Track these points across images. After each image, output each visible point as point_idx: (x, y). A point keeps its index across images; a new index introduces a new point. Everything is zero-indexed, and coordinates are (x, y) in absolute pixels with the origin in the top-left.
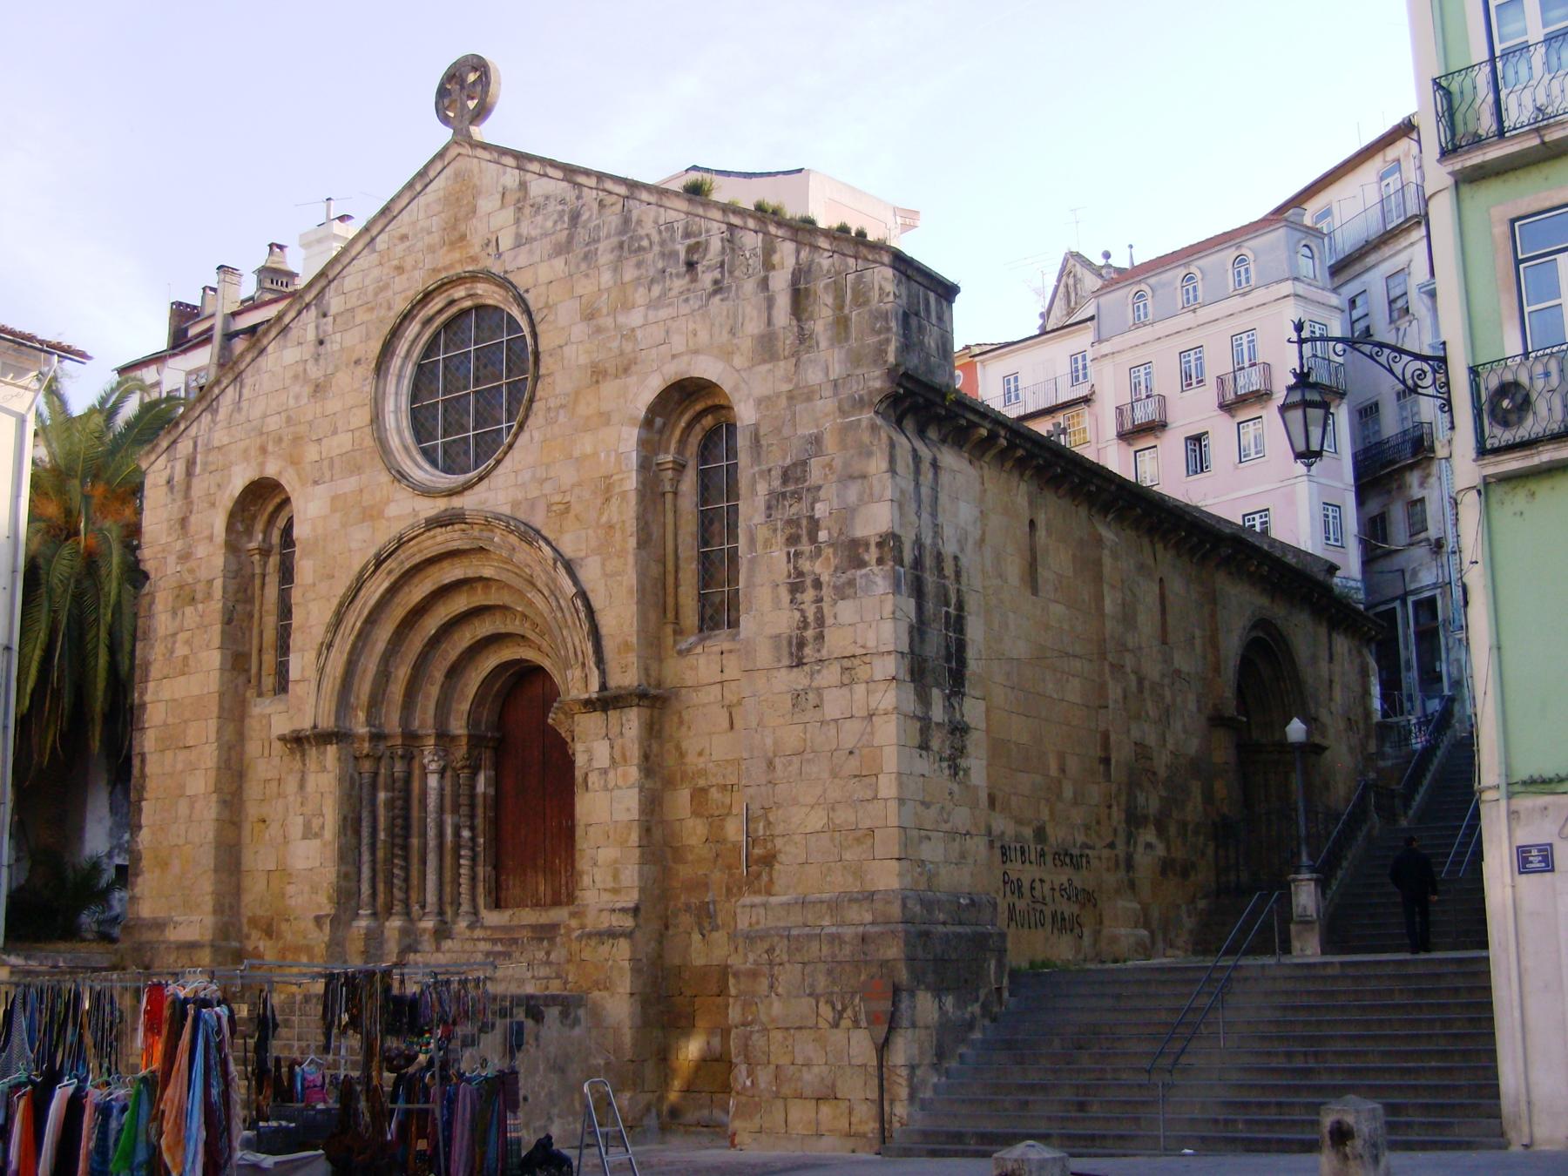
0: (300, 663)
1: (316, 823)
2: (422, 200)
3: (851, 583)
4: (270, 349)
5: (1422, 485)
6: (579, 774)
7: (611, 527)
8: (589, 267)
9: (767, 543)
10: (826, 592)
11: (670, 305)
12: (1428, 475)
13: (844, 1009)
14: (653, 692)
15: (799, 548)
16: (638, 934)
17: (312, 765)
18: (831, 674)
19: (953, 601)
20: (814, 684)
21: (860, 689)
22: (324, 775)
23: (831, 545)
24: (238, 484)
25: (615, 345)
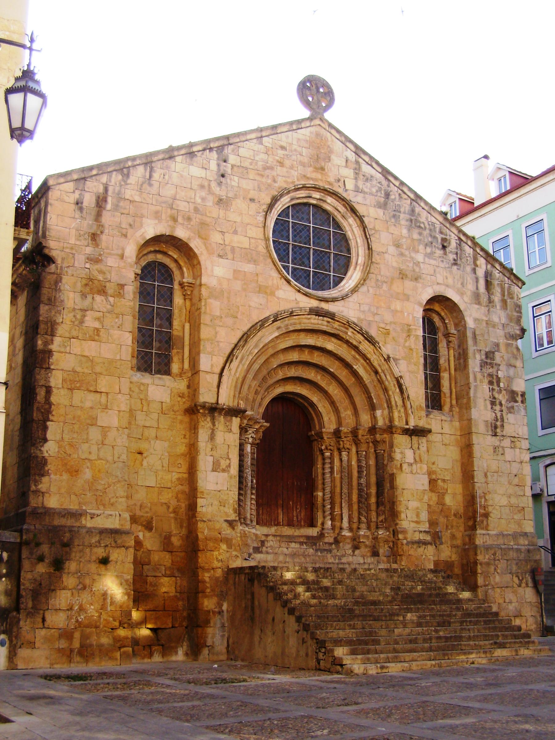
1: (224, 464)
2: (294, 133)
3: (513, 407)
7: (411, 349)
8: (396, 221)
9: (481, 381)
11: (435, 259)
13: (523, 579)
18: (507, 443)
20: (501, 445)
21: (517, 450)
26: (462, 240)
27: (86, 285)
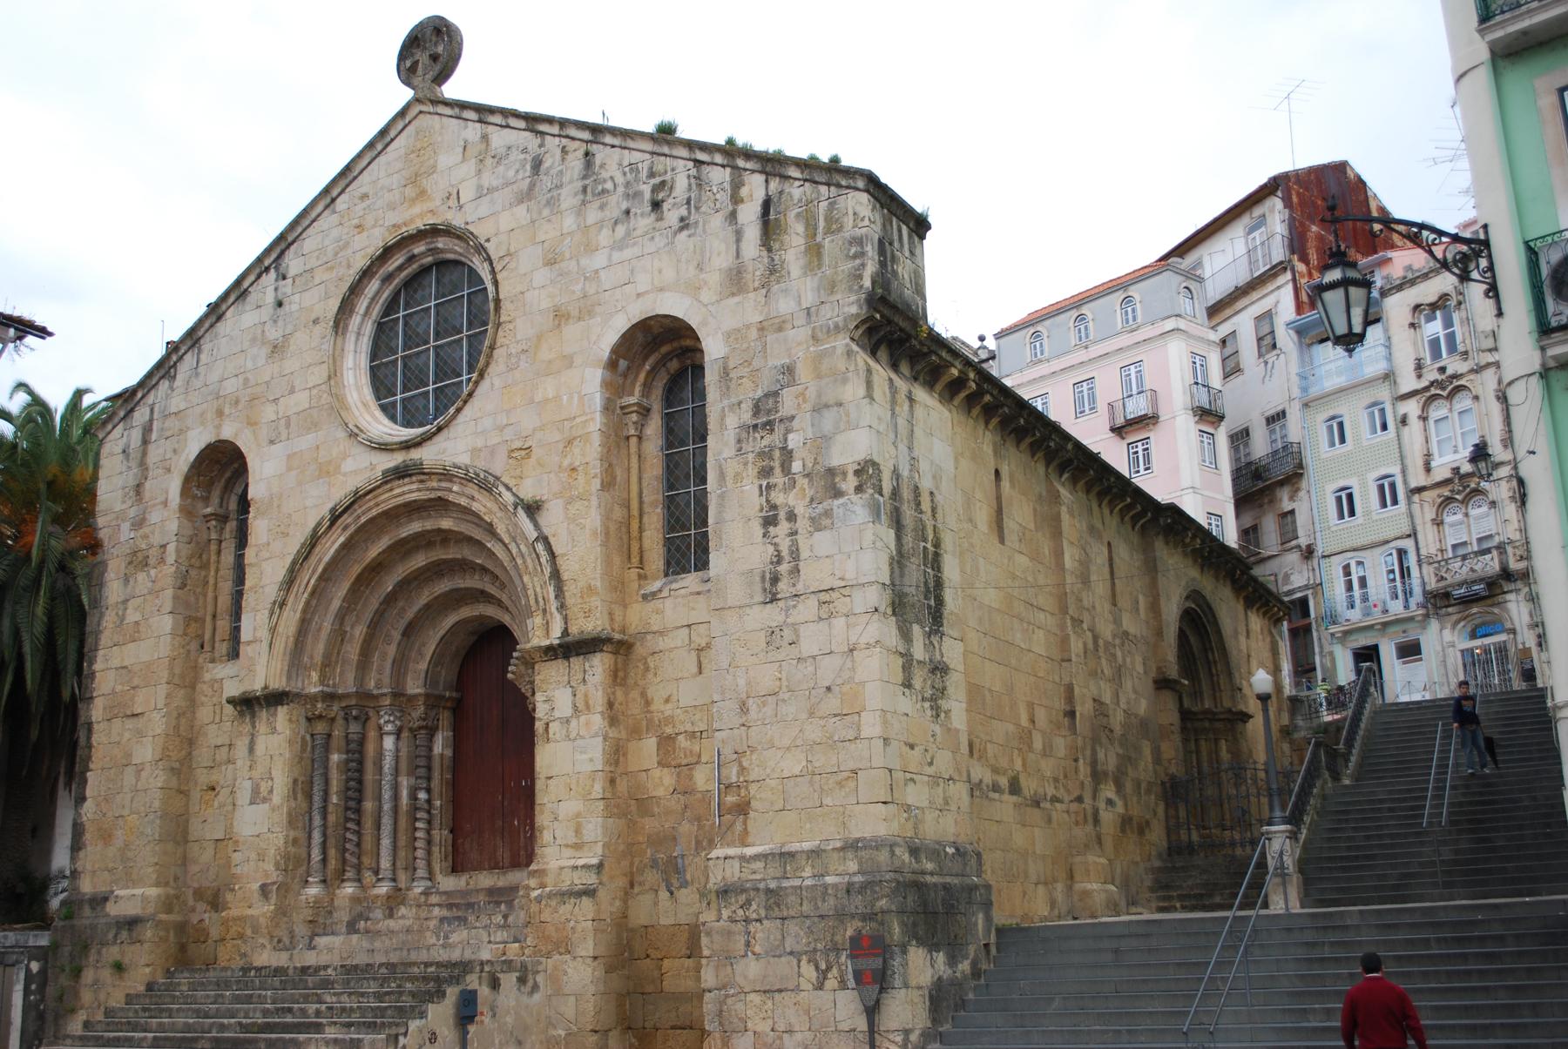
0: (253, 624)
2: (382, 158)
3: (828, 513)
4: (229, 314)
5: (1292, 499)
6: (539, 726)
9: (738, 477)
10: (802, 524)
12: (1298, 490)
13: (829, 968)
14: (617, 636)
15: (772, 480)
16: (601, 893)
17: (262, 727)
18: (807, 609)
19: (931, 537)
21: (839, 623)
22: (277, 737)
23: (807, 475)
24: (194, 445)
25: (580, 286)
26: (703, 163)
27: (130, 563)
